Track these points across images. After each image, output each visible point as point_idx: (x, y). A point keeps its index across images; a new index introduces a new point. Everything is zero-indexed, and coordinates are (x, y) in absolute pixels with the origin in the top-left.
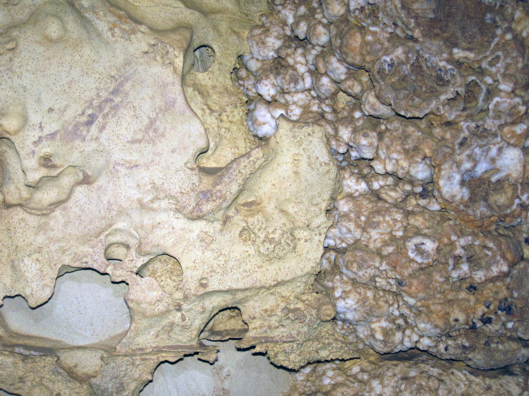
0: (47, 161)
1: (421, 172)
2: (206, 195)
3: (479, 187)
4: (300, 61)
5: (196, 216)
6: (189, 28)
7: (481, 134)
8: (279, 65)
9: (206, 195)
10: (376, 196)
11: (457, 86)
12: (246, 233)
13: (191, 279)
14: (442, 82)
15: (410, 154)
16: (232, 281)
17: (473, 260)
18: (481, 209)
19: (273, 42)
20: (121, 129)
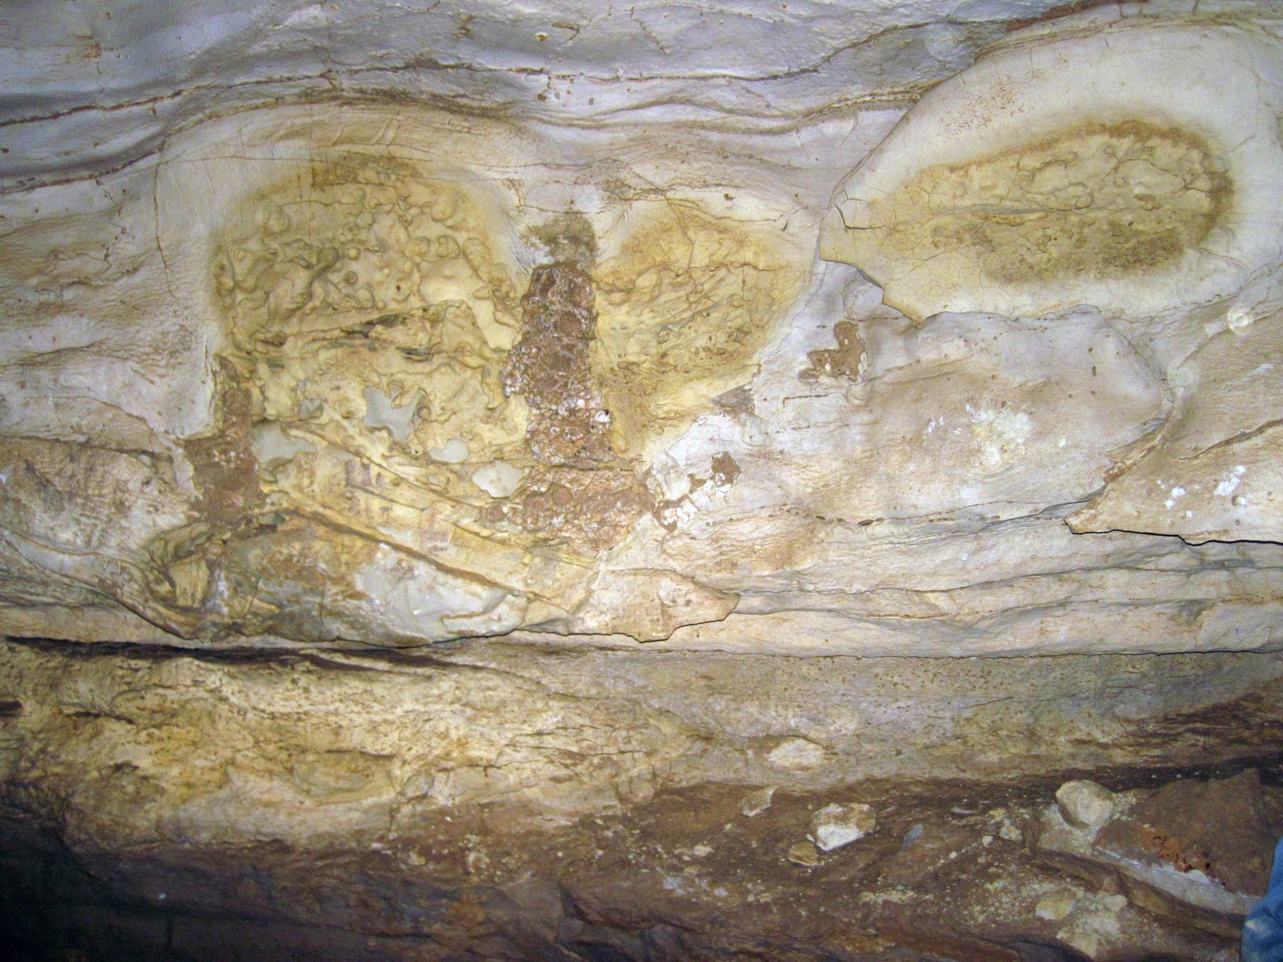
0: (443, 409)
1: (554, 407)
2: (489, 417)
3: (572, 412)
4: (518, 374)
5: (486, 423)
6: (482, 366)
7: (570, 396)
8: (511, 375)
9: (489, 417)
10: (542, 415)
11: (561, 383)
12: (503, 428)
13: (486, 442)
14: (556, 382)
15: (550, 402)
16: (499, 441)
17: (572, 434)
18: (572, 419)
19: (509, 368)
20: (464, 398)
